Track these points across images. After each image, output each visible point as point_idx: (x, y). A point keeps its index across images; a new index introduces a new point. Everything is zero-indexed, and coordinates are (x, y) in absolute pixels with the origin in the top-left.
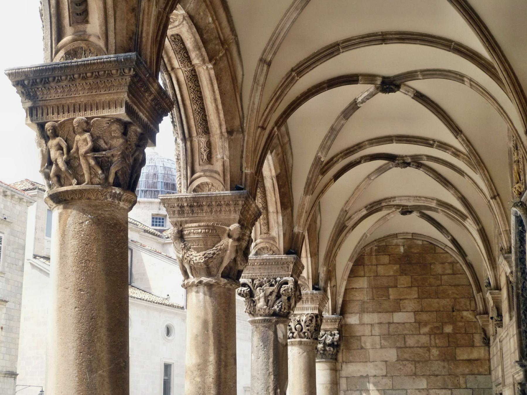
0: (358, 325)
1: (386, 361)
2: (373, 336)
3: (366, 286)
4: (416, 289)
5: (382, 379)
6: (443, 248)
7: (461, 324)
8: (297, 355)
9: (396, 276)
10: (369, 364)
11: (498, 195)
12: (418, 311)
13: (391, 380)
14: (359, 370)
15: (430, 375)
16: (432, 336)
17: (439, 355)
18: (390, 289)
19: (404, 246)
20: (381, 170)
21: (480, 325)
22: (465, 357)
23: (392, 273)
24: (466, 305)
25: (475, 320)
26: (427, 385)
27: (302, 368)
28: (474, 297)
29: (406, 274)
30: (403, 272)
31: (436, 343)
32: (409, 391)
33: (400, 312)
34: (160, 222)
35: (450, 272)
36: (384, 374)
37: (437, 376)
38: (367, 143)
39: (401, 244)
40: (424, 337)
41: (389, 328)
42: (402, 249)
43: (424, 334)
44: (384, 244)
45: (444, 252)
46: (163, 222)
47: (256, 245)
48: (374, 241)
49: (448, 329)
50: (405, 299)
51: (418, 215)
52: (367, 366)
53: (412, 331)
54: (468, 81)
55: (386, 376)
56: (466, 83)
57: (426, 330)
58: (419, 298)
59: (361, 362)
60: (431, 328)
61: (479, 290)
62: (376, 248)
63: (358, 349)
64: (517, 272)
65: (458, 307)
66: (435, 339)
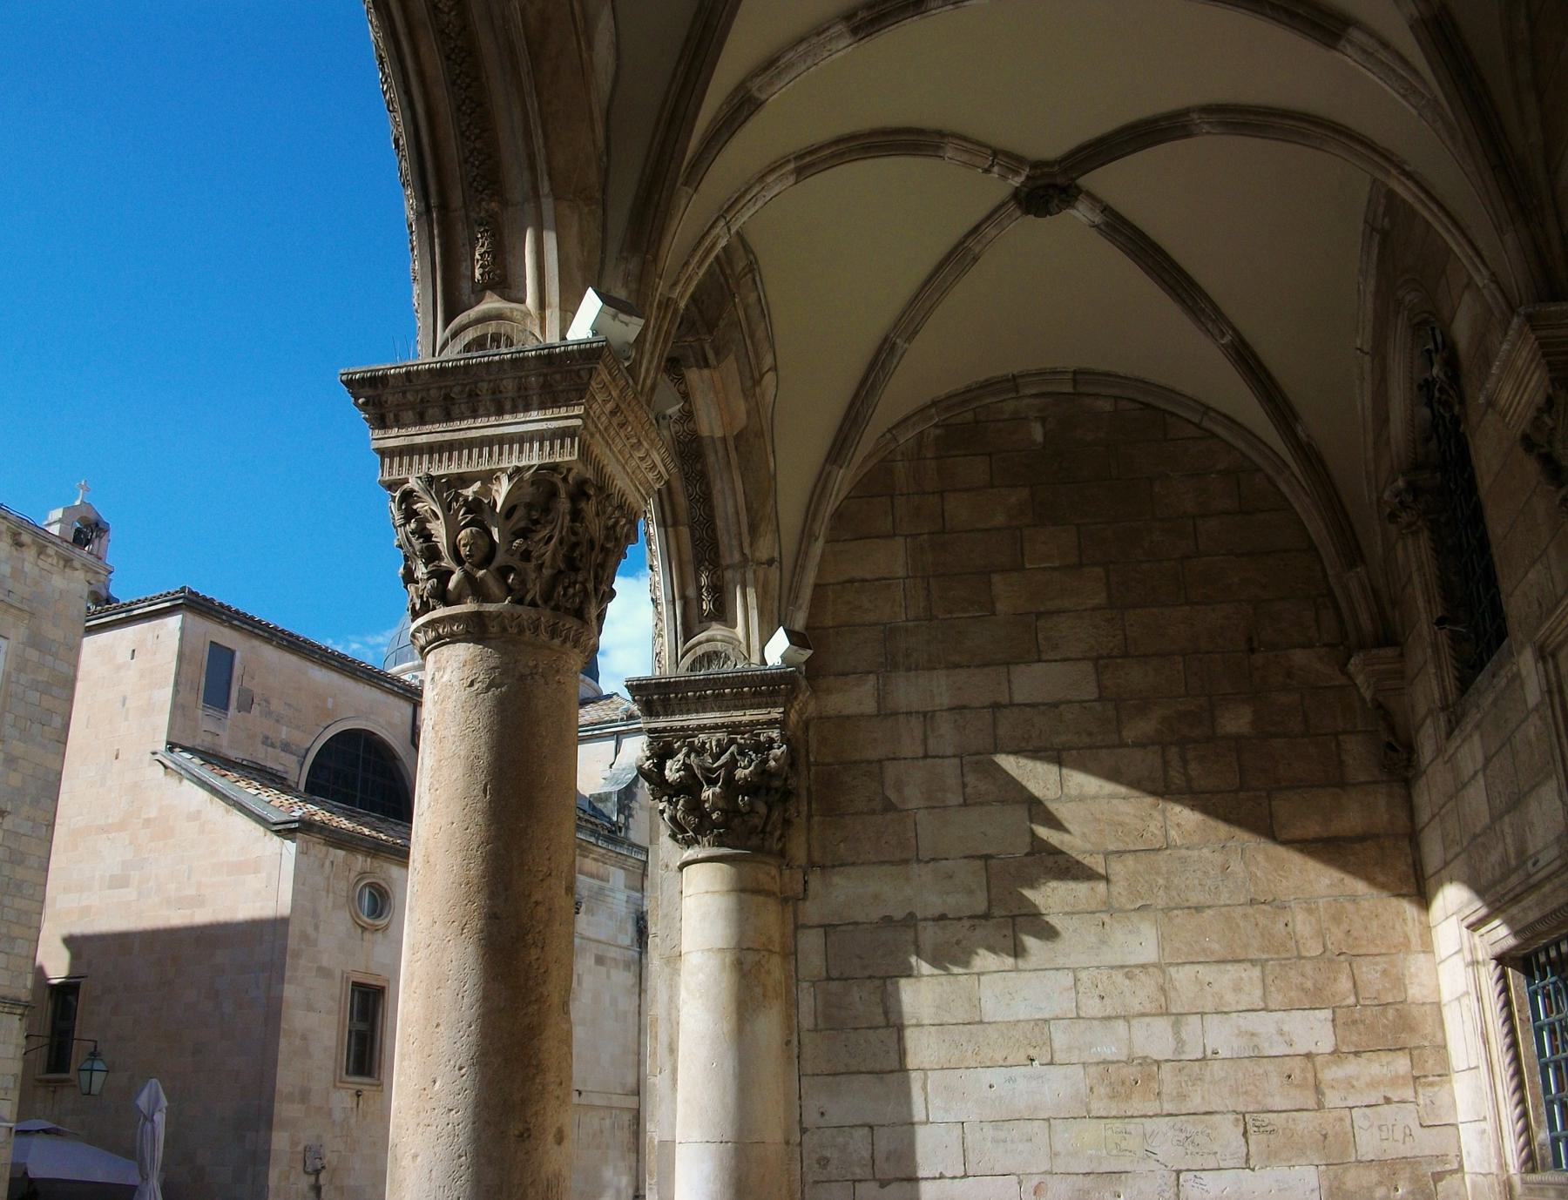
0: (871, 716)
1: (987, 858)
2: (929, 761)
3: (901, 572)
4: (1098, 570)
5: (973, 927)
6: (1196, 420)
8: (459, 694)
10: (915, 868)
12: (1109, 656)
13: (1009, 932)
14: (876, 897)
15: (1167, 910)
16: (1173, 752)
18: (996, 578)
19: (1043, 420)
21: (1363, 700)
23: (1000, 519)
25: (1342, 680)
26: (1161, 947)
27: (483, 763)
32: (1083, 975)
33: (1039, 661)
36: (981, 907)
37: (1198, 909)
41: (995, 725)
42: (1037, 433)
44: (969, 416)
48: (929, 407)
49: (1236, 721)
50: (1059, 612)
51: (1098, 218)
53: (1090, 734)
55: (986, 916)
59: (883, 862)
62: (938, 431)
63: (873, 812)
66: (1185, 762)
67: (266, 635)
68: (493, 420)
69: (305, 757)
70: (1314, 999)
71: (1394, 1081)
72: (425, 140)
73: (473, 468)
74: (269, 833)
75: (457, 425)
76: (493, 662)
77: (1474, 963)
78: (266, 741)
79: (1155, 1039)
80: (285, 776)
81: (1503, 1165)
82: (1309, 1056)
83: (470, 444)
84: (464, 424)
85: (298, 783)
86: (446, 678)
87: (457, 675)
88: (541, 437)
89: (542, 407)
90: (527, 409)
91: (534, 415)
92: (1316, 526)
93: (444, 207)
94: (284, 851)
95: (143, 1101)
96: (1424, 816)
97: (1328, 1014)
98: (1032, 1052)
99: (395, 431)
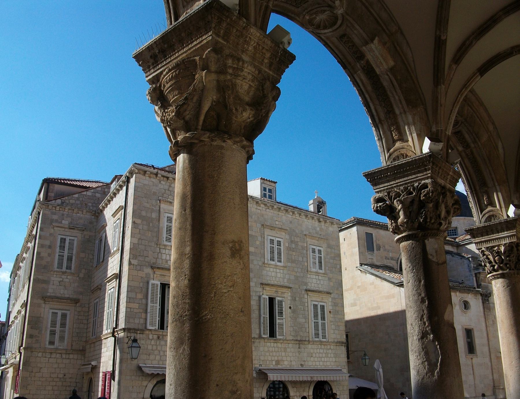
8: (501, 289)
34: (453, 233)
46: (455, 232)
47: (390, 155)
67: (380, 227)
68: (497, 234)
69: (398, 261)
72: (469, 178)
73: (495, 244)
74: (395, 286)
75: (490, 236)
76: (507, 282)
78: (386, 258)
80: (393, 267)
83: (493, 240)
84: (491, 236)
85: (397, 269)
86: (498, 286)
87: (500, 285)
88: (508, 237)
89: (507, 231)
90: (504, 231)
91: (506, 233)
93: (475, 190)
94: (401, 291)
95: (375, 366)
99: (477, 239)
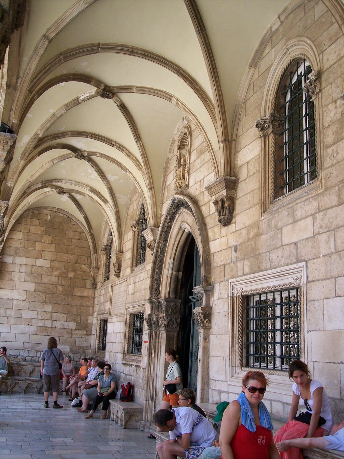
0: (11, 263)
3: (20, 238)
4: (54, 245)
5: (22, 302)
6: (76, 221)
7: (79, 272)
9: (42, 235)
10: (15, 291)
11: (154, 187)
12: (53, 260)
13: (28, 304)
14: (7, 295)
15: (54, 304)
16: (60, 278)
17: (62, 291)
18: (37, 243)
19: (50, 215)
20: (64, 158)
21: (91, 275)
22: (79, 294)
23: (39, 232)
24: (85, 261)
25: (89, 271)
26: (52, 310)
28: (91, 256)
29: (49, 235)
30: (47, 233)
31: (62, 283)
32: (39, 312)
33: (41, 259)
35: (78, 238)
36: (24, 299)
37: (59, 304)
38: (70, 133)
39: (49, 214)
40: (54, 278)
41: (32, 269)
42: (49, 218)
43: (55, 276)
45: (76, 224)
48: (31, 209)
49: (71, 275)
50: (46, 251)
51: (68, 196)
52: (13, 292)
53: (47, 273)
54: (176, 100)
56: (173, 102)
57: (56, 273)
58: (55, 252)
60: (60, 273)
61: (96, 252)
62: (32, 213)
63: (9, 280)
64: (160, 240)
65: (79, 261)
66: (62, 281)
70: (74, 321)
71: (83, 335)
77: (97, 320)
79: (48, 324)
81: (95, 349)
82: (71, 329)
92: (91, 245)
96: (96, 296)
97: (75, 323)
98: (29, 324)
